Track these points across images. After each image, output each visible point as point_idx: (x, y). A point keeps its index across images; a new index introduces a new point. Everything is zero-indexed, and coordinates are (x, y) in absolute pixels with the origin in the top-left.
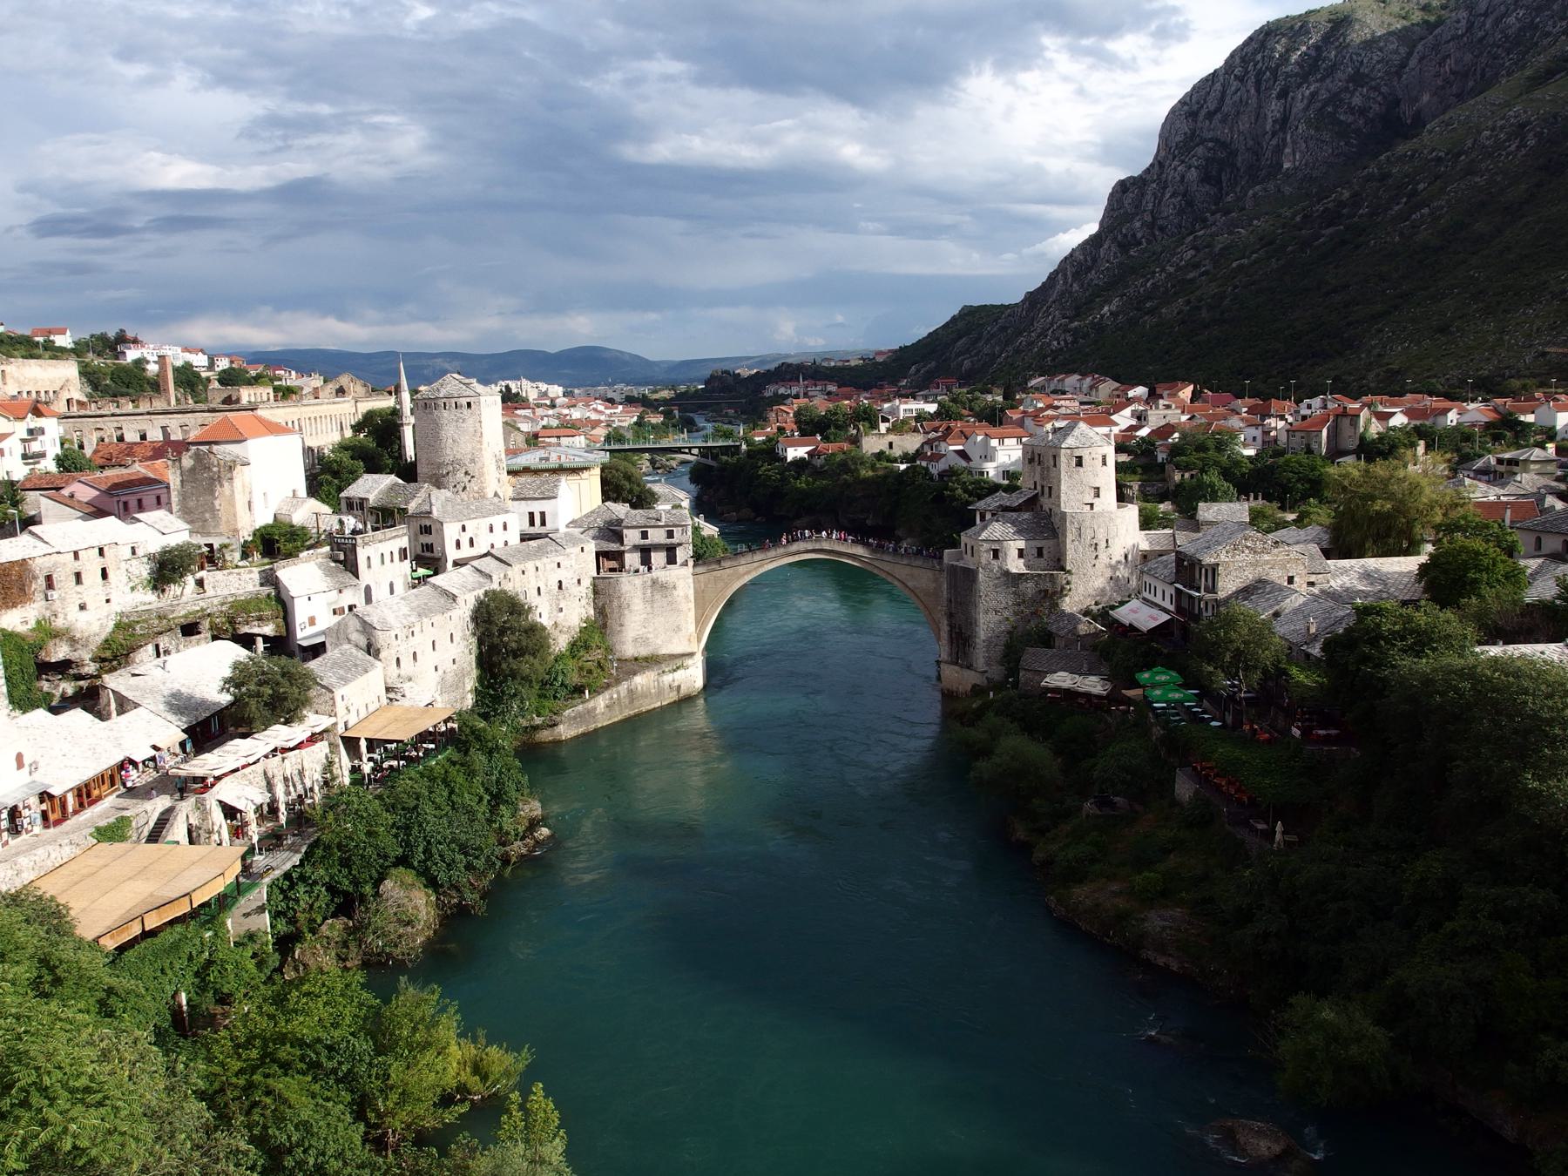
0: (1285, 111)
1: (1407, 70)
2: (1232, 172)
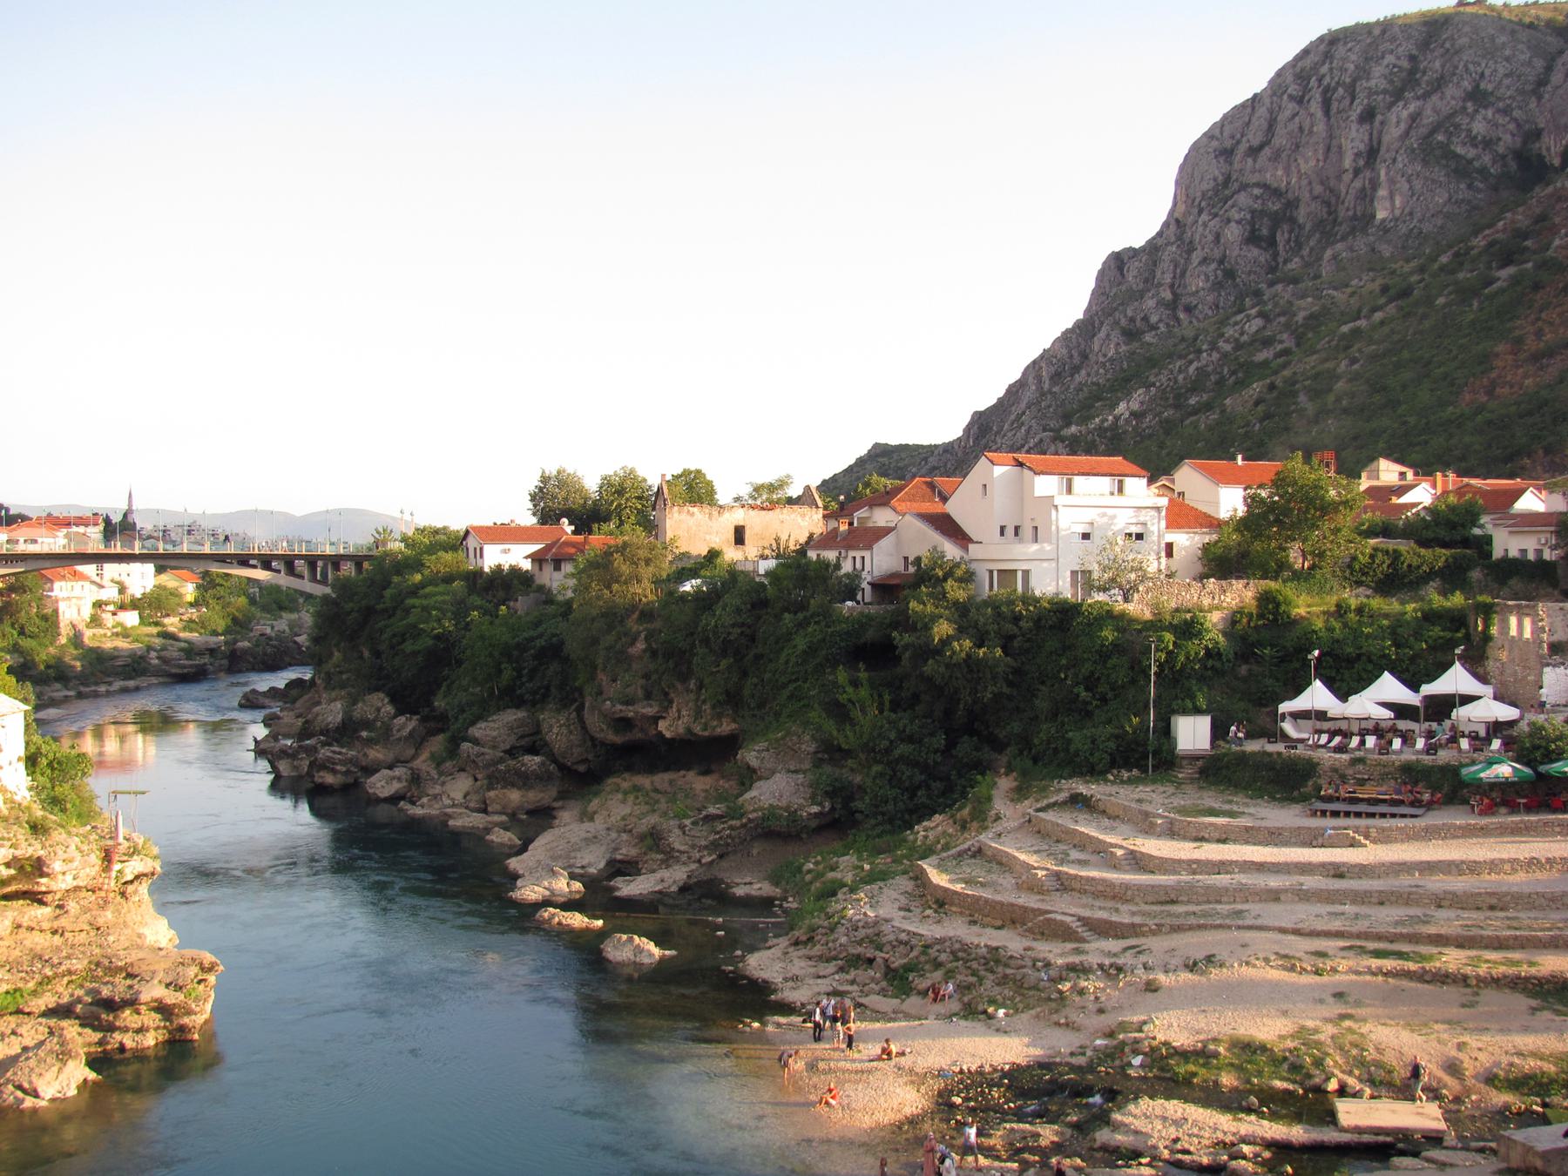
0: (1371, 139)
1: (1549, 88)
2: (1290, 232)
